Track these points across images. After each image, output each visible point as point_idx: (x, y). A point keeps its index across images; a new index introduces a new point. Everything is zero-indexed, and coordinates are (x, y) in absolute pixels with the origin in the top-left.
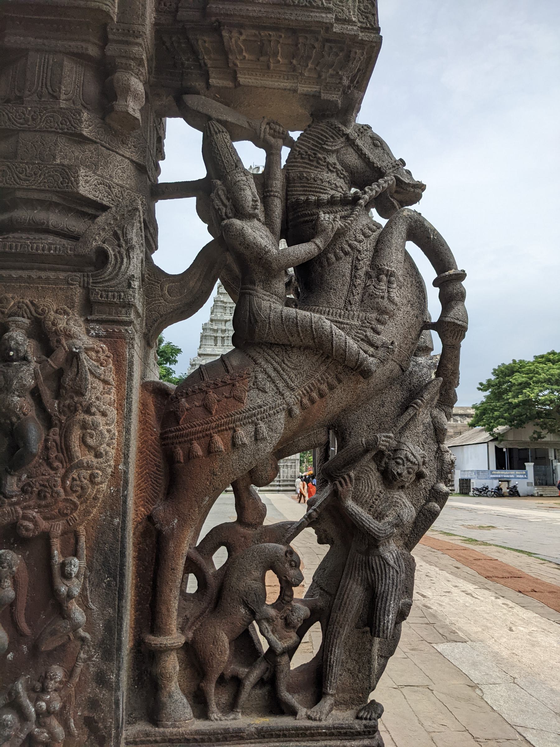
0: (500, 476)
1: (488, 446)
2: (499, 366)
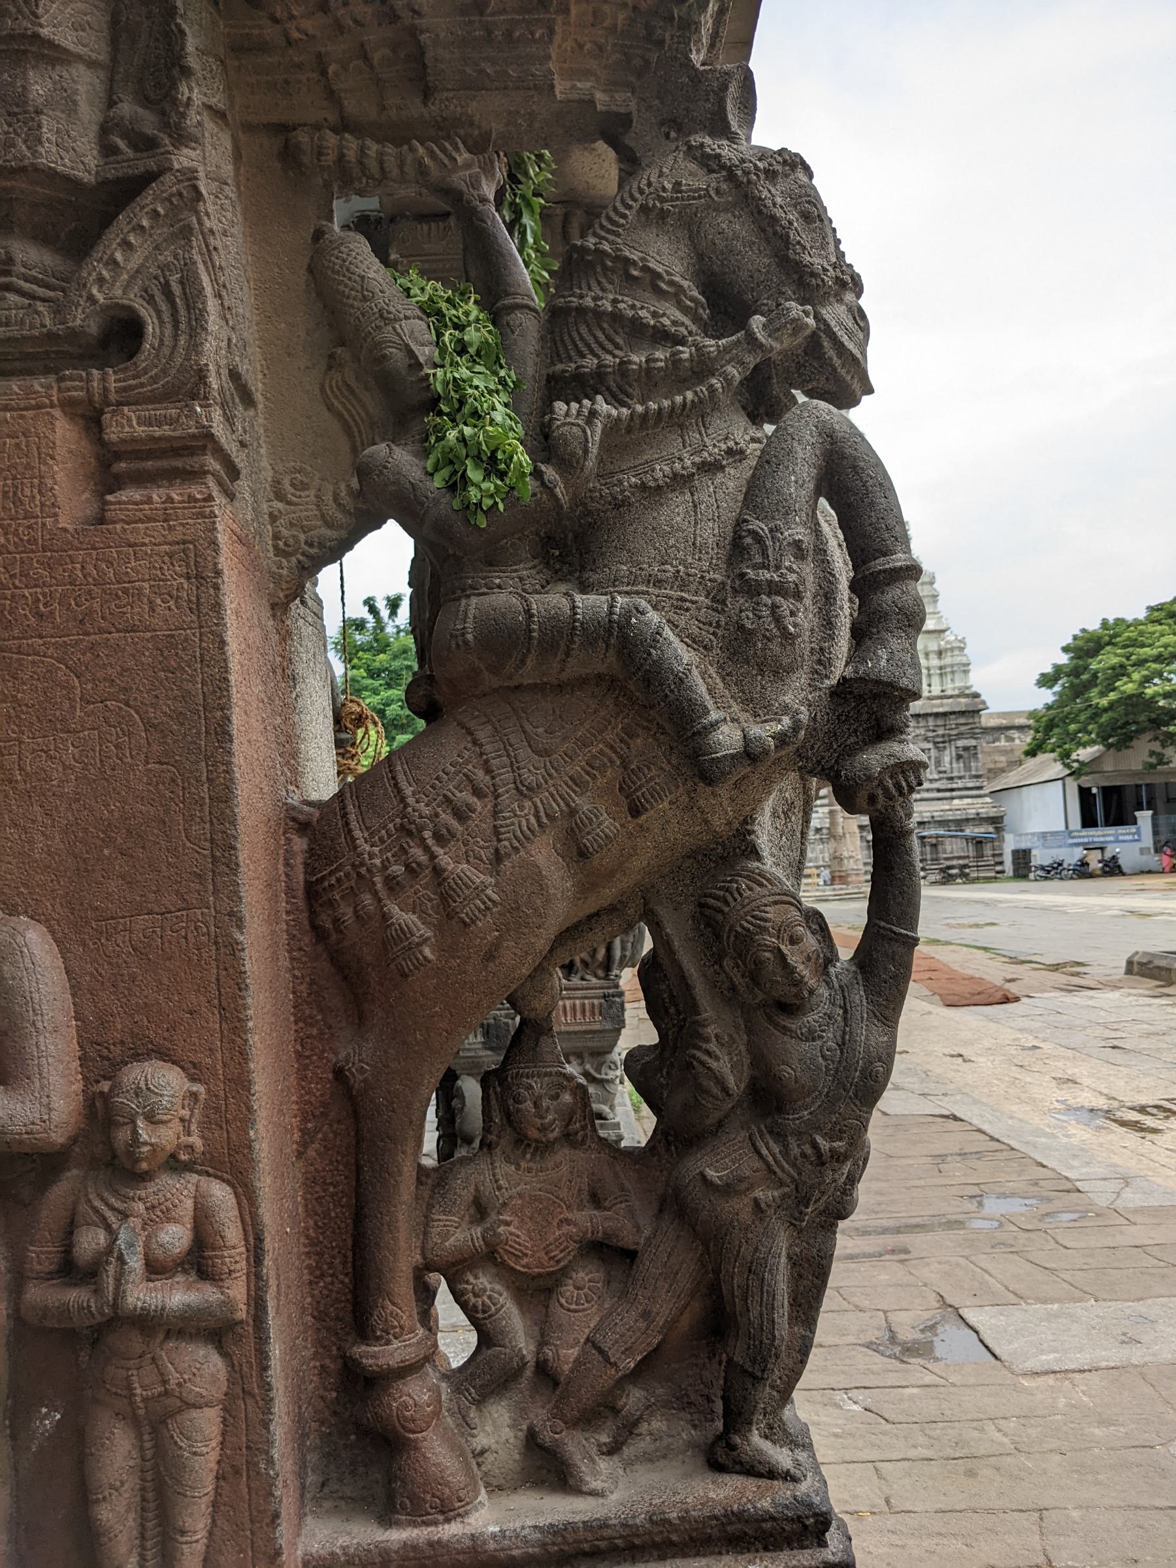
0: (1086, 840)
1: (1064, 785)
2: (1075, 638)
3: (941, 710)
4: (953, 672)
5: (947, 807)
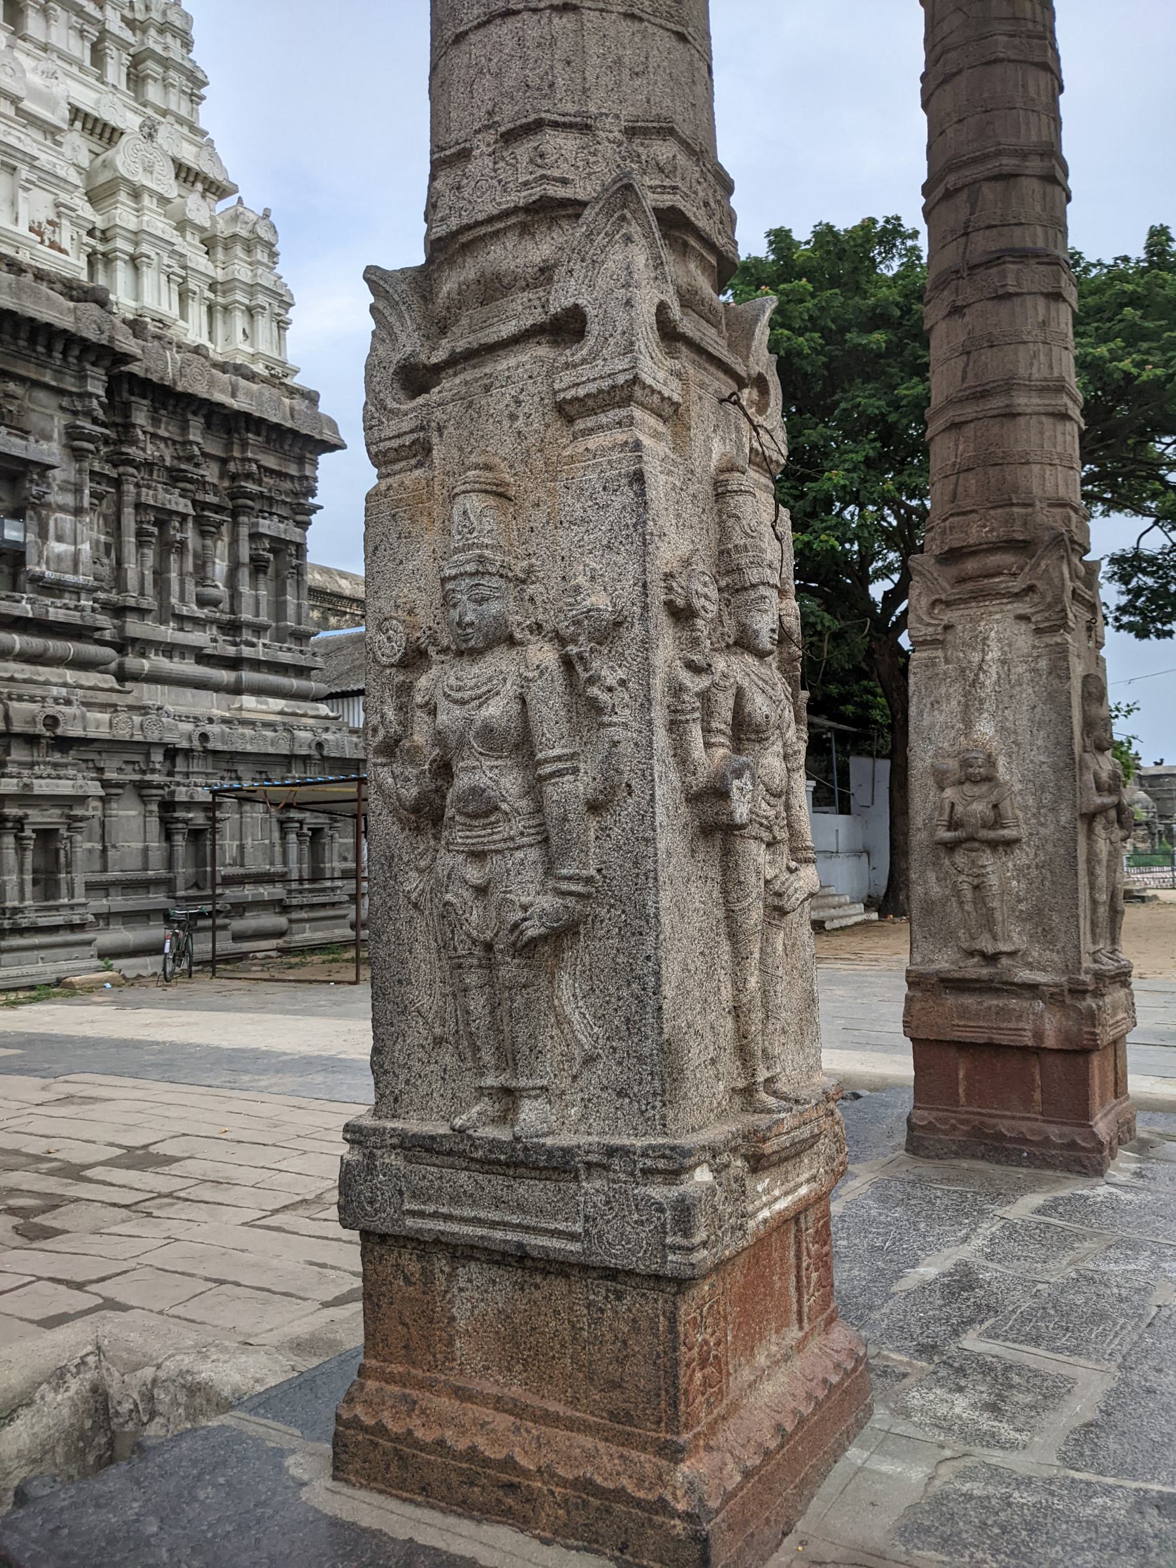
4: (250, 312)
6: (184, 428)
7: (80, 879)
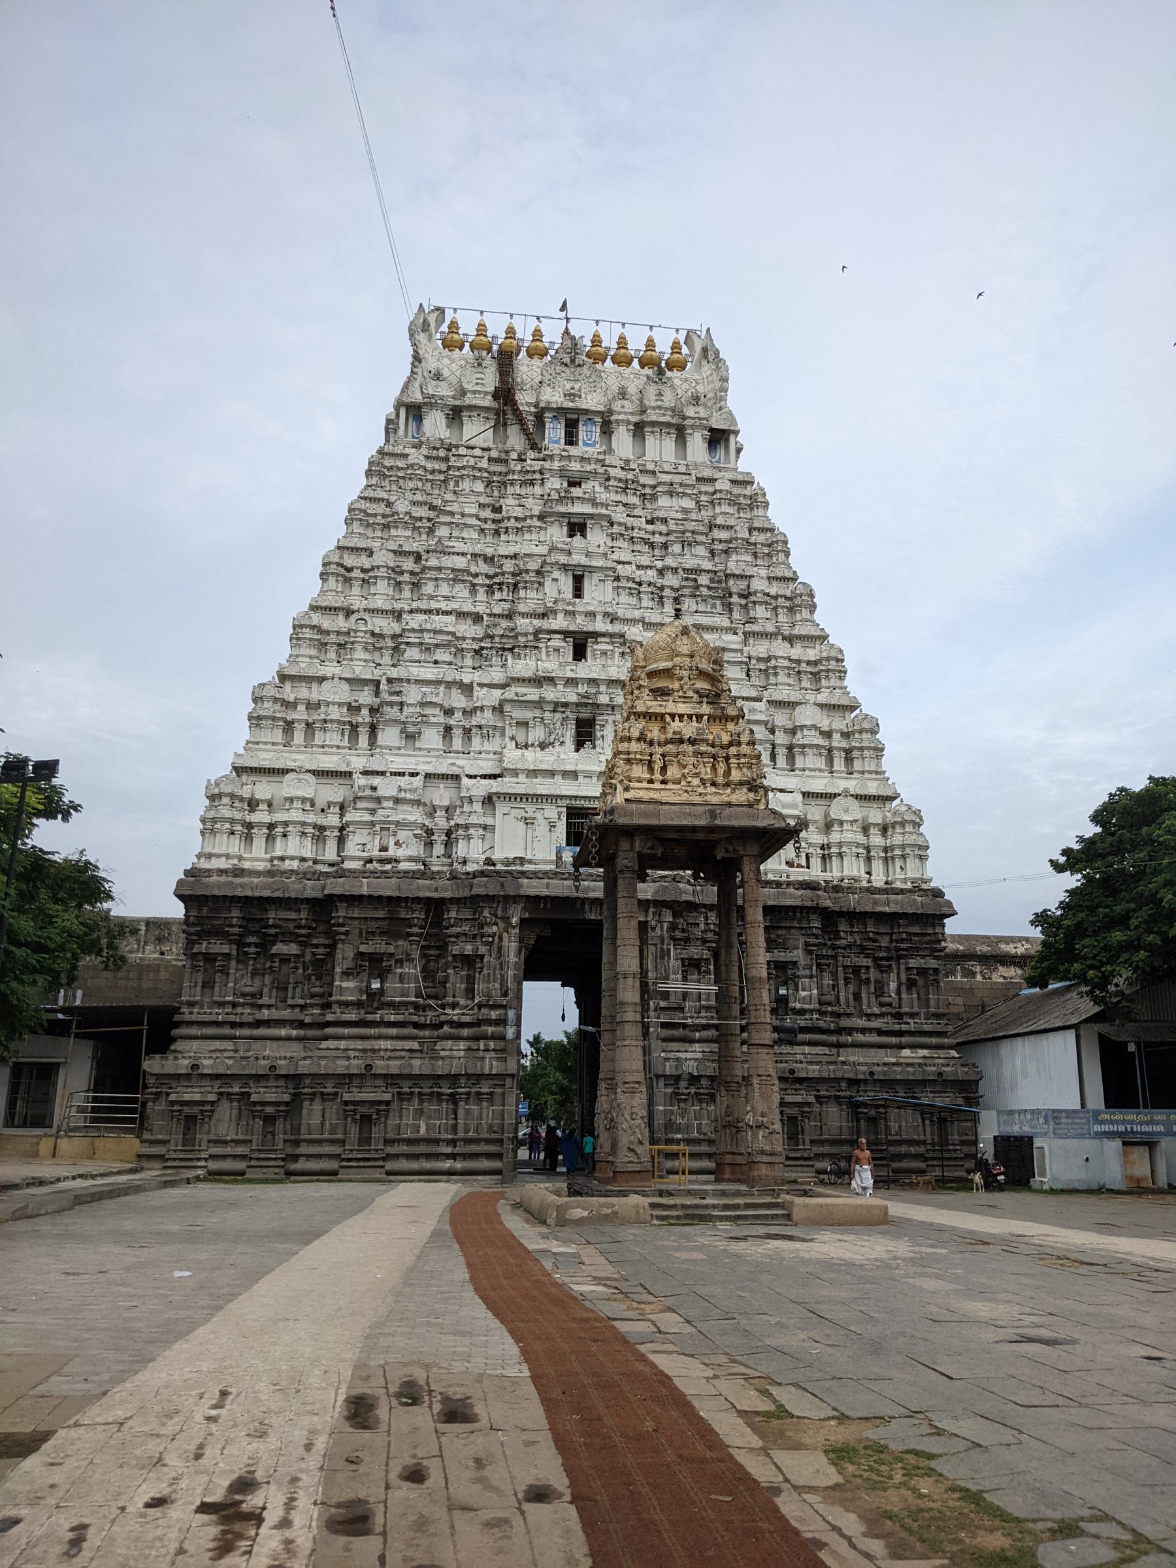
3: (887, 909)
4: (904, 857)
5: (893, 1060)
6: (865, 926)
7: (807, 1138)
